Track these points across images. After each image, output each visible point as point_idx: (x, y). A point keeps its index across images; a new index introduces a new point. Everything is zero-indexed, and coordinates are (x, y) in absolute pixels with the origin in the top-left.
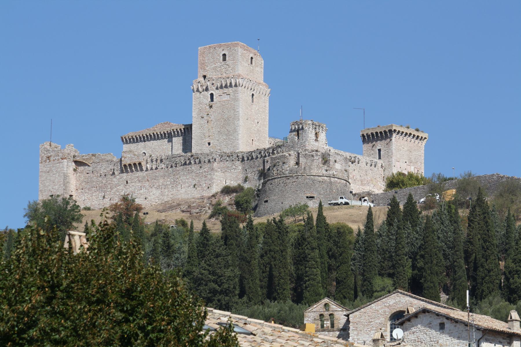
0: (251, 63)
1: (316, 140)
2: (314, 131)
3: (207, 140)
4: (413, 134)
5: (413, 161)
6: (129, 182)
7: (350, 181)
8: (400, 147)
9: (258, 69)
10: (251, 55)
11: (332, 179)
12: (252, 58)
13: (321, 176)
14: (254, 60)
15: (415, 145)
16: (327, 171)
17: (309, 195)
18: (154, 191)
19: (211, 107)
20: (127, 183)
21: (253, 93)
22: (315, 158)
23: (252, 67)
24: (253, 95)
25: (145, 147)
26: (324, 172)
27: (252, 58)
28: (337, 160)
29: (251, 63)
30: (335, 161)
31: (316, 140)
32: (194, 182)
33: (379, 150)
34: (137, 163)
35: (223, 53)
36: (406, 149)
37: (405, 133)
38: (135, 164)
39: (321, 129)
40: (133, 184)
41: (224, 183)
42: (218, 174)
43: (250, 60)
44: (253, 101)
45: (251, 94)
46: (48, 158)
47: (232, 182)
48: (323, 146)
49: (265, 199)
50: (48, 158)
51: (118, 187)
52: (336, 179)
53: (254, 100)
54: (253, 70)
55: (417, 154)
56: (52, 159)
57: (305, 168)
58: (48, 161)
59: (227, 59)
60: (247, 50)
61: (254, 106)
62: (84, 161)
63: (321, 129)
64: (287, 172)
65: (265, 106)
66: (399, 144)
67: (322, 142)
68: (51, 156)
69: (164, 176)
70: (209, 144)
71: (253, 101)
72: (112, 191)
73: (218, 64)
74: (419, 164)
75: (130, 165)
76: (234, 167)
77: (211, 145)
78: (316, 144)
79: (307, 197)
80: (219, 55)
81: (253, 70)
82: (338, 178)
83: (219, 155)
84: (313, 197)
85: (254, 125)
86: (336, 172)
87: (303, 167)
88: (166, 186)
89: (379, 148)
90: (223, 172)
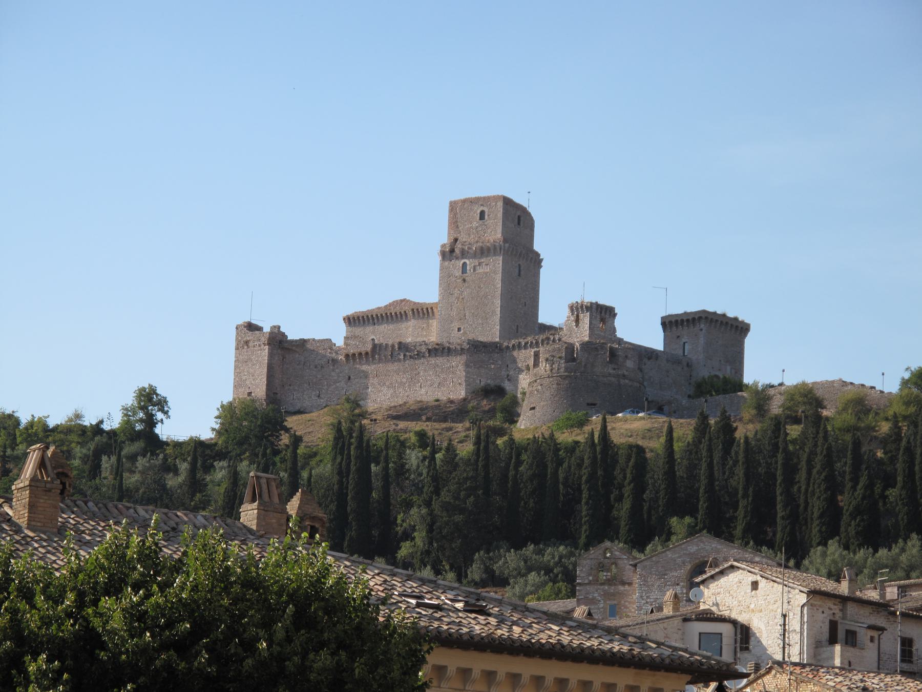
0: (519, 224)
2: (599, 317)
3: (456, 325)
4: (730, 323)
6: (352, 377)
7: (645, 383)
10: (519, 213)
11: (622, 381)
12: (519, 217)
13: (607, 377)
14: (522, 219)
16: (614, 369)
17: (590, 401)
18: (385, 389)
19: (464, 280)
20: (349, 378)
21: (520, 263)
22: (600, 352)
23: (519, 229)
24: (519, 265)
25: (373, 333)
26: (612, 371)
27: (519, 217)
28: (630, 356)
29: (519, 224)
30: (626, 357)
32: (437, 381)
33: (684, 343)
34: (363, 353)
35: (482, 208)
37: (720, 322)
38: (360, 354)
39: (608, 314)
40: (357, 380)
41: (478, 382)
42: (470, 370)
43: (517, 220)
44: (519, 275)
45: (517, 265)
46: (247, 343)
47: (489, 382)
48: (610, 337)
49: (532, 406)
50: (247, 343)
51: (338, 384)
52: (627, 381)
53: (522, 273)
56: (251, 344)
57: (585, 365)
58: (246, 347)
59: (486, 217)
62: (294, 348)
63: (608, 314)
64: (562, 370)
67: (610, 331)
68: (249, 340)
69: (397, 372)
70: (459, 330)
71: (519, 275)
72: (330, 389)
73: (475, 224)
75: (354, 355)
76: (491, 361)
77: (462, 331)
79: (588, 404)
80: (476, 212)
82: (630, 380)
83: (473, 345)
84: (594, 405)
85: (520, 306)
86: (627, 371)
87: (583, 364)
88: (402, 384)
89: (684, 340)
90: (478, 368)
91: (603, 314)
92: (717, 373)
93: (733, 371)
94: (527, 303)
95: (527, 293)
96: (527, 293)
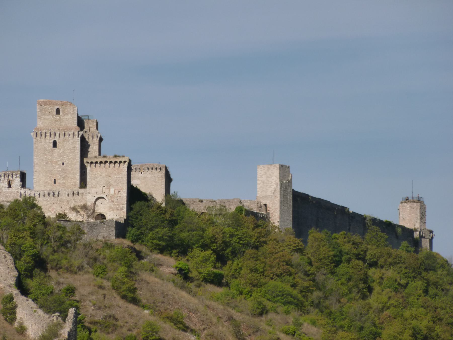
1: (10, 186)
2: (6, 180)
4: (109, 161)
5: (113, 183)
8: (96, 175)
9: (69, 116)
14: (61, 110)
15: (115, 169)
21: (55, 139)
23: (58, 117)
31: (10, 186)
36: (104, 175)
39: (14, 177)
43: (55, 112)
45: (52, 141)
48: (17, 191)
54: (60, 119)
55: (118, 177)
60: (50, 104)
61: (56, 150)
65: (75, 147)
66: (95, 173)
67: (16, 187)
74: (121, 185)
78: (10, 190)
81: (60, 119)
85: (58, 167)
91: (10, 178)
92: (101, 196)
93: (117, 191)
94: (65, 164)
95: (65, 156)
96: (65, 156)
